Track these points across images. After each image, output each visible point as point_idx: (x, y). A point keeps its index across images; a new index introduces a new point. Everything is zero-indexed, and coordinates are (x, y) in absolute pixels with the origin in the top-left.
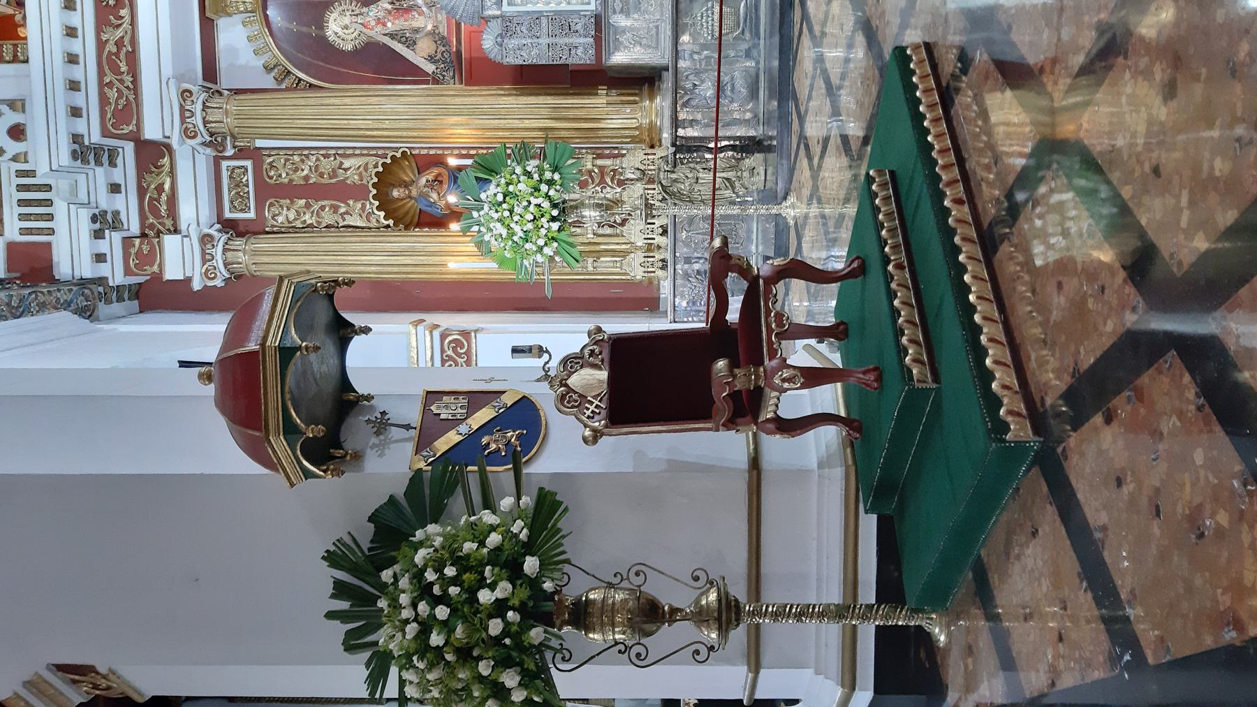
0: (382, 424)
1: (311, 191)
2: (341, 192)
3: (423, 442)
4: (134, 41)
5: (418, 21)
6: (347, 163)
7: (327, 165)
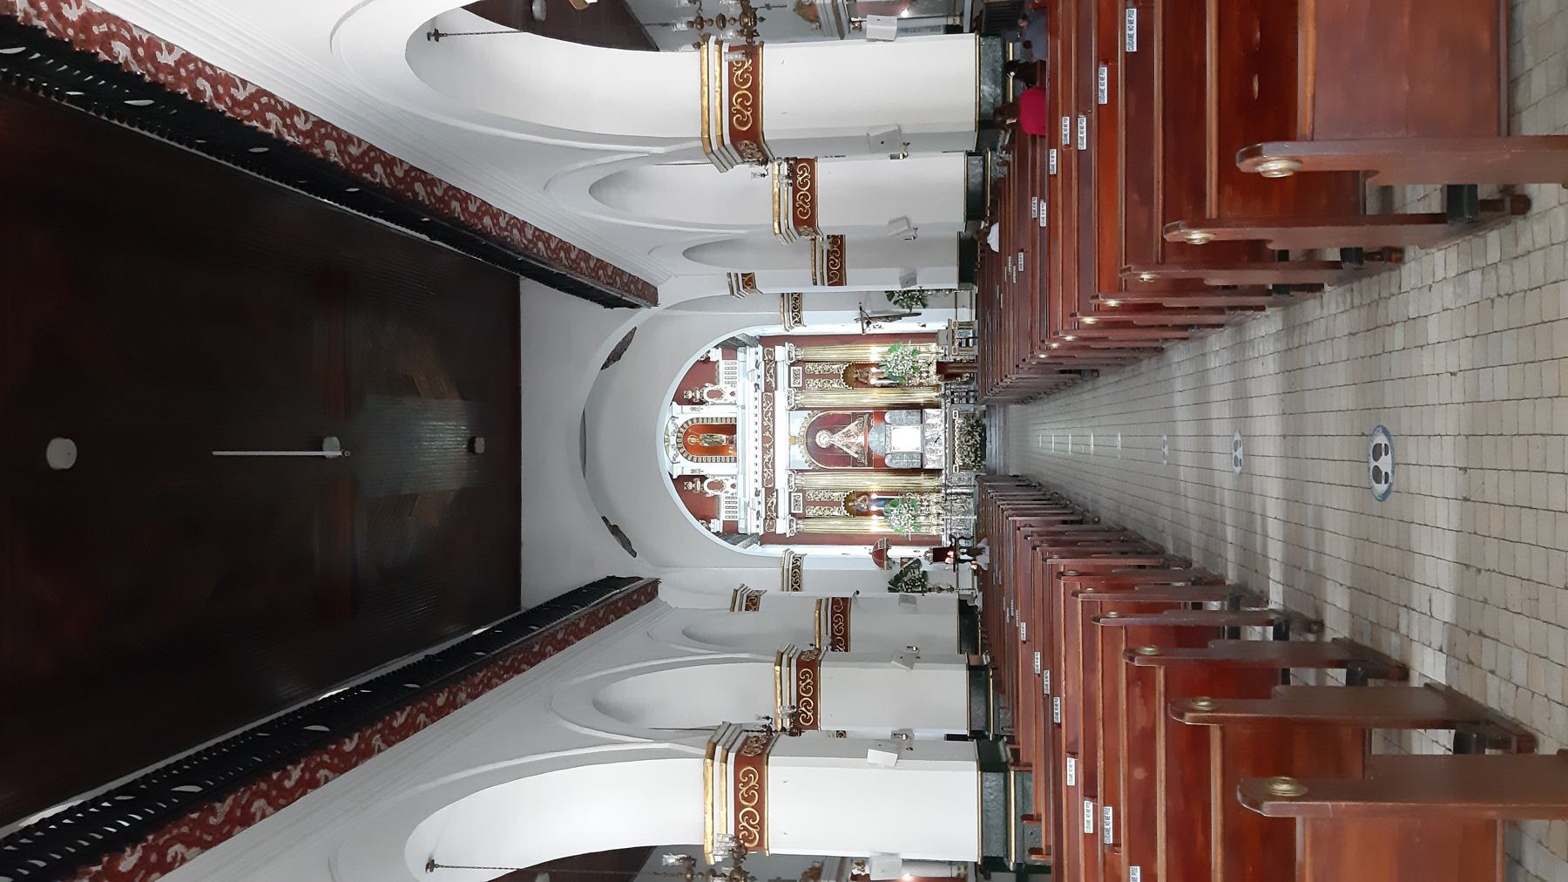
0: (894, 562)
1: (821, 503)
2: (832, 504)
3: (902, 565)
5: (853, 440)
7: (827, 495)
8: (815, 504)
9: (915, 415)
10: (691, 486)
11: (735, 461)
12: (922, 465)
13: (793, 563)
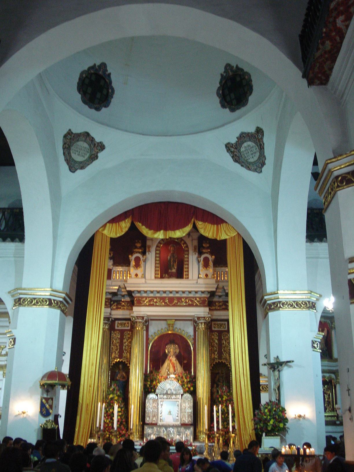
4: (156, 306)
6: (128, 354)
8: (122, 339)
9: (188, 420)
10: (139, 245)
11: (155, 278)
12: (148, 424)
13: (54, 300)
